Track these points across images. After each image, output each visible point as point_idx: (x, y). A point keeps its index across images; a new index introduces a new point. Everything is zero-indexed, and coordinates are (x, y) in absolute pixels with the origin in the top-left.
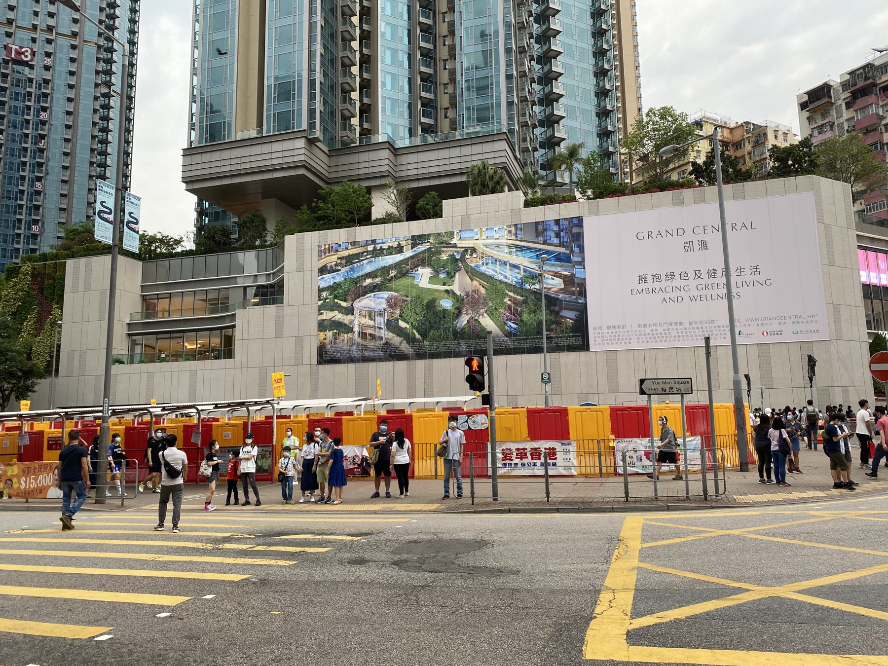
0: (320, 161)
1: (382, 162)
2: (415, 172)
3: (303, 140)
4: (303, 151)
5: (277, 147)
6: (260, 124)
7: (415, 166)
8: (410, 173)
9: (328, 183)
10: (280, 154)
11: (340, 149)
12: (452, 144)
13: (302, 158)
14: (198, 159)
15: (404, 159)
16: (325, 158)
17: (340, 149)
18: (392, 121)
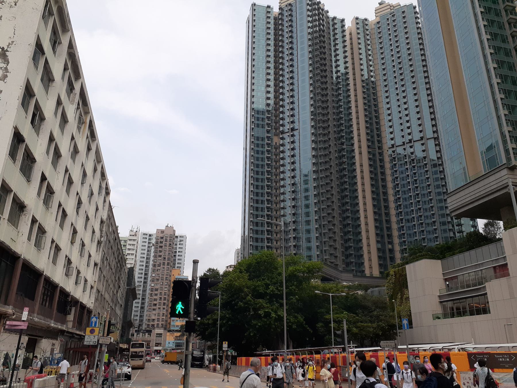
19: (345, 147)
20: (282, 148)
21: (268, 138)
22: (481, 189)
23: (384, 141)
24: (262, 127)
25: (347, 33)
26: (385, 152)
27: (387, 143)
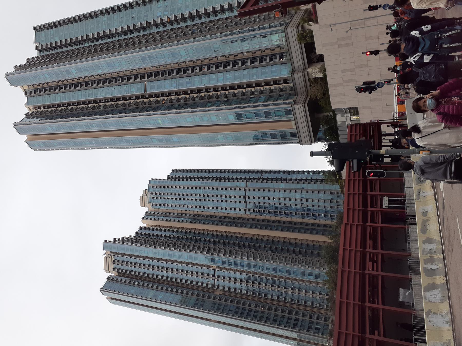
0: (301, 98)
2: (301, 62)
3: (295, 105)
4: (299, 105)
5: (298, 114)
6: (290, 120)
10: (301, 113)
13: (301, 105)
14: (303, 140)
15: (296, 68)
16: (299, 97)
17: (294, 91)
19: (237, 242)
20: (227, 289)
21: (214, 298)
23: (239, 216)
24: (204, 302)
26: (247, 217)
27: (242, 214)
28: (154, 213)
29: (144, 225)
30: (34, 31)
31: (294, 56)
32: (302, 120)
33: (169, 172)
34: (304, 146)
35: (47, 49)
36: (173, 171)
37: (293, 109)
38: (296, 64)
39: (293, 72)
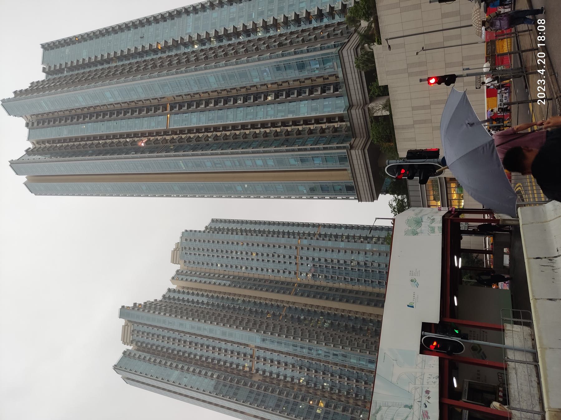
0: (359, 142)
1: (358, 113)
2: (361, 95)
5: (355, 162)
6: (345, 170)
7: (357, 96)
8: (361, 98)
9: (369, 137)
10: (359, 161)
11: (351, 133)
12: (346, 78)
13: (360, 151)
14: (363, 196)
15: (354, 102)
16: (358, 140)
17: (351, 133)
18: (332, 106)
20: (268, 374)
22: (362, 176)
25: (182, 290)
28: (187, 272)
29: (174, 287)
30: (41, 50)
31: (352, 87)
32: (361, 170)
33: (207, 222)
34: (364, 203)
35: (56, 72)
36: (213, 221)
37: (350, 155)
38: (354, 98)
39: (350, 106)
